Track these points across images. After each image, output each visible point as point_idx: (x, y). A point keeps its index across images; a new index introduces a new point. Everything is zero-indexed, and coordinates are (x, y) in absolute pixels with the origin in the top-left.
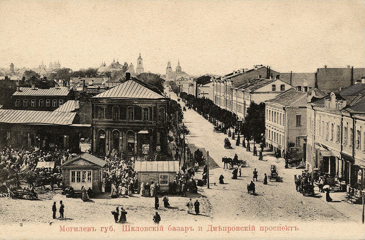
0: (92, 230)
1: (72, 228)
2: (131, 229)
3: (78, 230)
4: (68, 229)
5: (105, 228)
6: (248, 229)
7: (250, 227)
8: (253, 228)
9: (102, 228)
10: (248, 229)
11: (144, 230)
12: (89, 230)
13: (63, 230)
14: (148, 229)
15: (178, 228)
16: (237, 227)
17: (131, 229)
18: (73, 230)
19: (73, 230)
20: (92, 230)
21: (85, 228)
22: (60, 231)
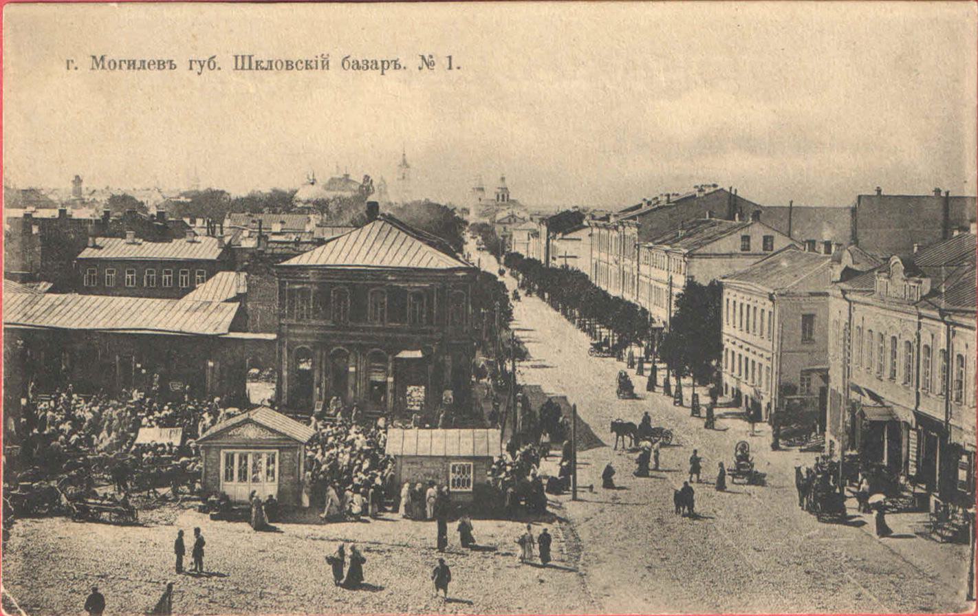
0: (167, 66)
1: (123, 63)
2: (254, 65)
3: (136, 67)
4: (112, 63)
5: (200, 62)
6: (313, 64)
7: (317, 61)
8: (325, 63)
9: (191, 61)
10: (313, 64)
11: (285, 67)
12: (162, 67)
13: (101, 66)
14: (294, 65)
15: (290, 67)
16: (287, 62)
17: (254, 65)
18: (125, 66)
19: (125, 66)
20: (167, 66)
21: (152, 63)
22: (93, 69)
